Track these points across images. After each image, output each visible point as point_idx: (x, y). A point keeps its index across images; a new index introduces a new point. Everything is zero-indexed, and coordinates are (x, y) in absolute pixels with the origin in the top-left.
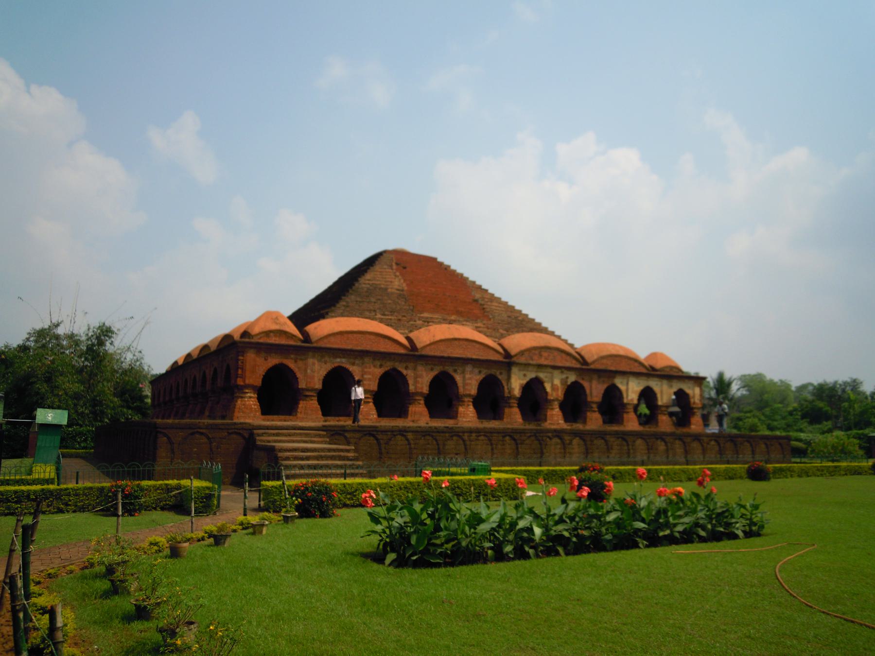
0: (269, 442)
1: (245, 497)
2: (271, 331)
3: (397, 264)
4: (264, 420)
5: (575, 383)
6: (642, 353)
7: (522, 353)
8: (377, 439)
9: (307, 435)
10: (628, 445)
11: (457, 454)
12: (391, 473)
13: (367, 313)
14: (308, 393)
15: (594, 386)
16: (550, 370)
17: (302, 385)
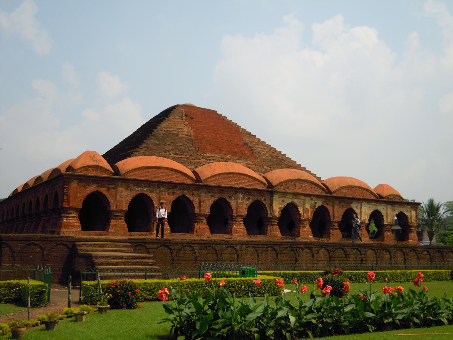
0: (88, 251)
1: (69, 293)
2: (89, 166)
3: (186, 115)
4: (84, 234)
5: (322, 207)
6: (372, 185)
7: (281, 184)
8: (170, 249)
9: (116, 246)
10: (361, 254)
11: (231, 261)
12: (180, 275)
13: (163, 153)
14: (117, 214)
15: (335, 209)
16: (303, 197)
17: (113, 208)
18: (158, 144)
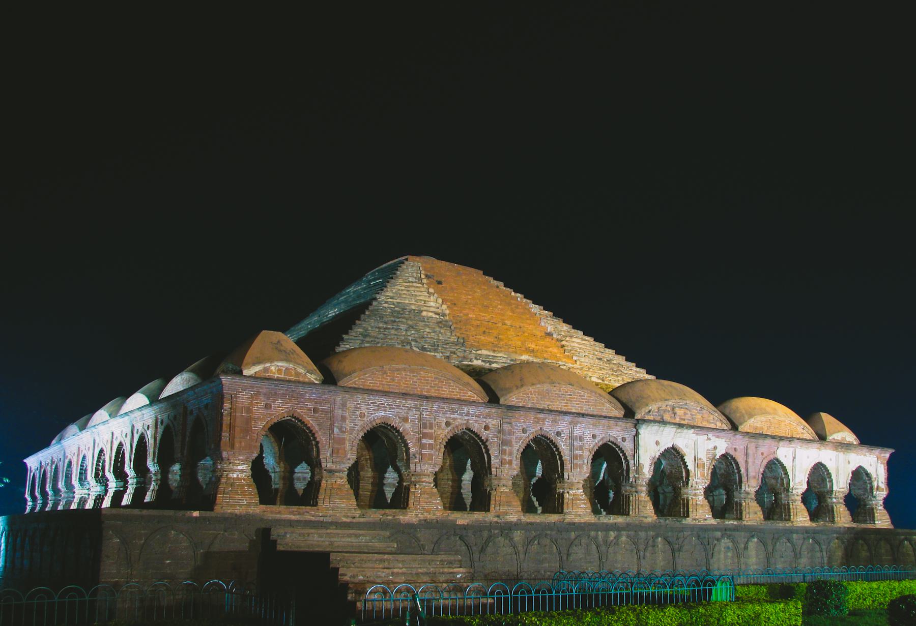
3: (426, 276)
18: (385, 329)
